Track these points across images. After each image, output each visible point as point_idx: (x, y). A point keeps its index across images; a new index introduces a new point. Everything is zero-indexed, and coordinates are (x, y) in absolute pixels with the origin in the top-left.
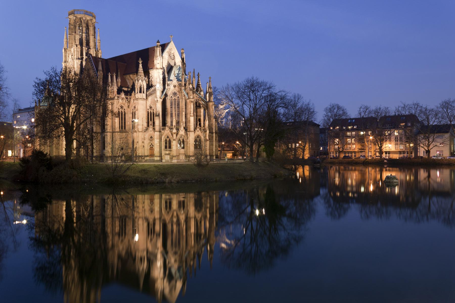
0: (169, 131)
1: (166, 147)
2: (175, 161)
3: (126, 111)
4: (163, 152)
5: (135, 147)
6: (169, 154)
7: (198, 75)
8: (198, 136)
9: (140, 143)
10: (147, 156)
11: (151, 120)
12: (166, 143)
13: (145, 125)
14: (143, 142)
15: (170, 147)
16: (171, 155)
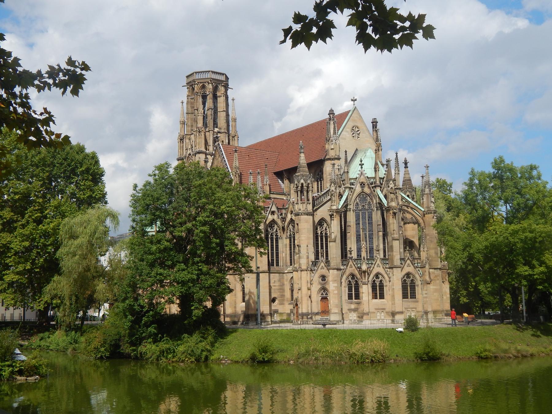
0: (354, 267)
1: (350, 297)
2: (367, 324)
3: (279, 234)
4: (345, 308)
5: (295, 297)
6: (355, 310)
7: (406, 163)
8: (408, 275)
9: (304, 289)
10: (317, 314)
11: (322, 248)
12: (350, 289)
13: (312, 257)
14: (309, 289)
15: (357, 297)
16: (360, 310)
